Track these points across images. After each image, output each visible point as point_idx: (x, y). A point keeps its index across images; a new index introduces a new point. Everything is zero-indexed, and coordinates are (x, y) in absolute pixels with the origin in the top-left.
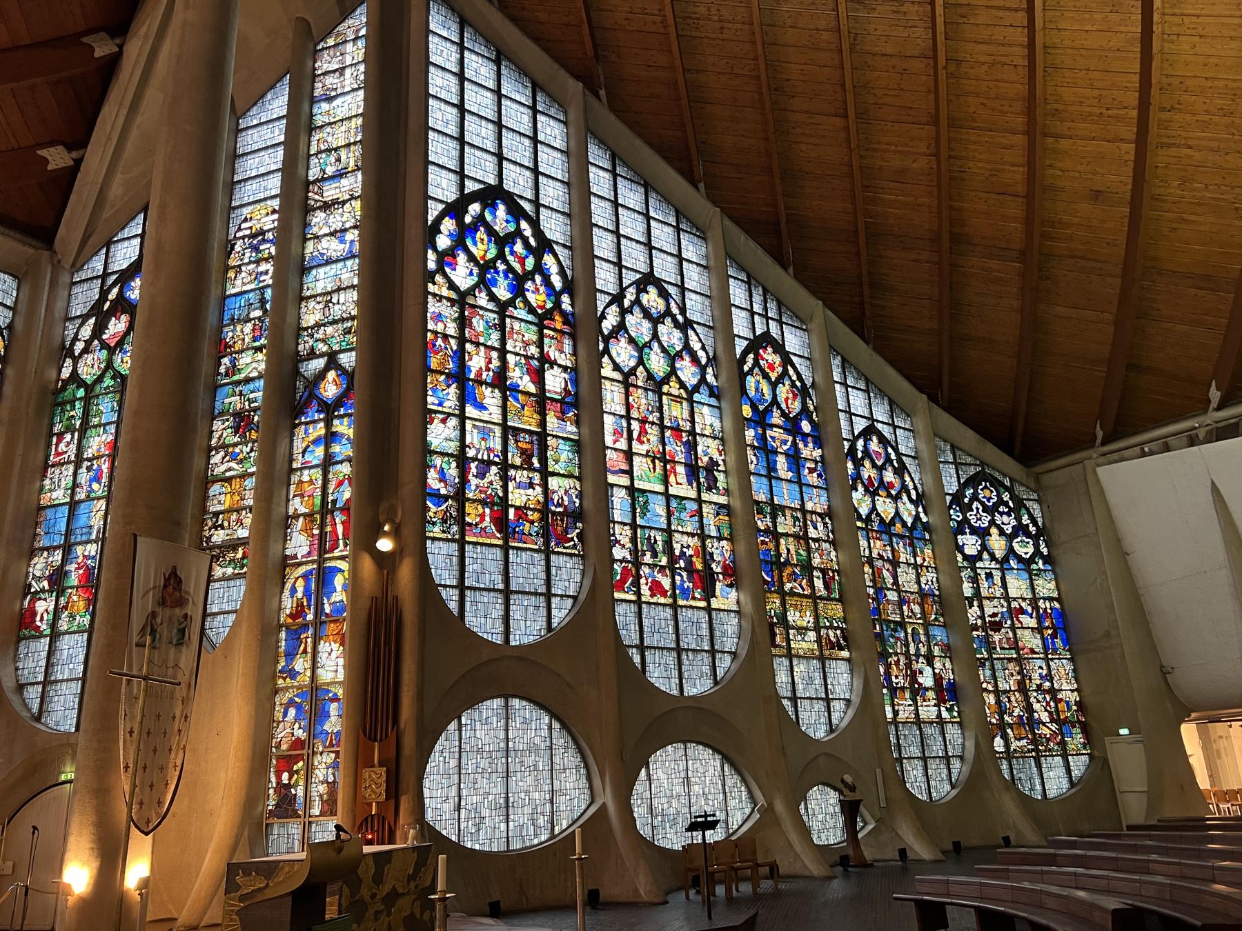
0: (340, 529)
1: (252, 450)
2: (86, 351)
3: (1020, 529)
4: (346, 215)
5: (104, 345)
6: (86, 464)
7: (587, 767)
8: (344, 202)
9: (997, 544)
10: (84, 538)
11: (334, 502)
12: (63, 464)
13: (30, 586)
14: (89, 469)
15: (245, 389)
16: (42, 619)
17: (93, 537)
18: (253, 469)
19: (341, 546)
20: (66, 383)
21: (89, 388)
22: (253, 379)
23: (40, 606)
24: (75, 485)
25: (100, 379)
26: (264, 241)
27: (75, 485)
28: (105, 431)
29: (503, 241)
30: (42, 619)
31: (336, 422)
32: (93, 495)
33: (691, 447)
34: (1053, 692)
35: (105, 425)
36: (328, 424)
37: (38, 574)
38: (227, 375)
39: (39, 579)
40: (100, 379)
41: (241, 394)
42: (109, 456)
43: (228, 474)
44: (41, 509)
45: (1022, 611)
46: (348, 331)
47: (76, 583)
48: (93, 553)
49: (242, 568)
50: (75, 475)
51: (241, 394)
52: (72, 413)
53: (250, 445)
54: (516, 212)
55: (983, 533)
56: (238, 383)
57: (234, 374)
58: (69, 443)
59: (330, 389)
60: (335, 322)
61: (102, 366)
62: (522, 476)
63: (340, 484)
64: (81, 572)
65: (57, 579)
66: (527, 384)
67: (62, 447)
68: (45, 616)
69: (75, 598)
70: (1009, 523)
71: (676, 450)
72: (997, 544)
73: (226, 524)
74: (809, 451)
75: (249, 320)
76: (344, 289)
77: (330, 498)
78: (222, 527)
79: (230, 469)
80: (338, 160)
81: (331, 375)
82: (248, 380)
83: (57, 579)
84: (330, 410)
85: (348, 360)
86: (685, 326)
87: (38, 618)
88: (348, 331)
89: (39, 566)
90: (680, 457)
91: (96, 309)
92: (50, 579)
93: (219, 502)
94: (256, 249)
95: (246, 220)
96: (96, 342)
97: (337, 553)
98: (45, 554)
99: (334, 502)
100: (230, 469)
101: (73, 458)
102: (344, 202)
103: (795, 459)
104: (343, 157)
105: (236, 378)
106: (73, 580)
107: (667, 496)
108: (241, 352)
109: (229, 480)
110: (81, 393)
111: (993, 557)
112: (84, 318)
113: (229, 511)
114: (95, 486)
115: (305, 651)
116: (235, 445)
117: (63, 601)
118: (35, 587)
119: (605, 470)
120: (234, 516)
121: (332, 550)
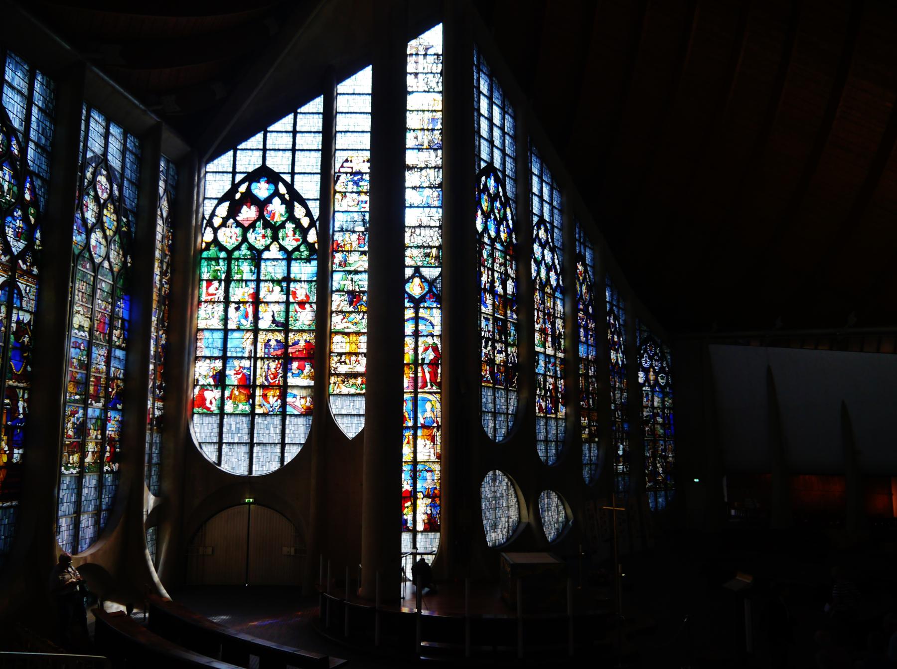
0: (428, 376)
1: (363, 318)
2: (224, 224)
3: (662, 370)
4: (423, 178)
5: (239, 224)
6: (233, 306)
7: (519, 504)
8: (422, 169)
9: (652, 377)
10: (240, 355)
11: (423, 359)
12: (214, 302)
13: (198, 380)
14: (237, 309)
15: (356, 277)
16: (211, 403)
18: (365, 330)
19: (429, 386)
21: (230, 253)
22: (361, 272)
24: (226, 319)
25: (238, 248)
26: (362, 179)
27: (226, 319)
28: (247, 286)
29: (493, 199)
30: (211, 403)
31: (421, 310)
32: (242, 327)
33: (553, 324)
34: (666, 457)
35: (246, 281)
36: (417, 312)
38: (340, 265)
40: (238, 248)
41: (352, 280)
42: (252, 303)
43: (346, 330)
44: (198, 330)
45: (658, 414)
46: (427, 255)
47: (236, 383)
49: (362, 389)
50: (226, 311)
51: (352, 280)
52: (217, 268)
53: (361, 314)
54: (497, 180)
55: (646, 371)
56: (350, 272)
57: (345, 266)
59: (415, 288)
60: (418, 247)
61: (240, 239)
62: (498, 346)
63: (426, 349)
64: (239, 376)
65: (220, 379)
66: (499, 290)
67: (212, 290)
68: (213, 401)
70: (657, 365)
71: (549, 326)
72: (652, 377)
73: (347, 361)
74: (592, 325)
75: (354, 232)
76: (425, 227)
77: (420, 357)
78: (346, 363)
79: (348, 328)
80: (416, 138)
81: (417, 280)
82: (356, 272)
83: (220, 379)
84: (417, 303)
85: (432, 273)
86: (552, 250)
88: (427, 255)
90: (549, 332)
91: (229, 196)
92: (214, 377)
93: (342, 347)
94: (356, 183)
95: (347, 161)
96: (231, 221)
97: (426, 389)
99: (423, 359)
100: (348, 328)
101: (222, 299)
102: (422, 169)
103: (586, 327)
104: (420, 138)
105: (347, 269)
107: (544, 353)
108: (350, 252)
109: (348, 334)
110: (223, 255)
111: (649, 386)
112: (221, 201)
113: (350, 354)
114: (243, 321)
115: (408, 443)
116: (350, 312)
117: (227, 393)
118: (202, 382)
119: (534, 345)
120: (353, 358)
121: (423, 387)
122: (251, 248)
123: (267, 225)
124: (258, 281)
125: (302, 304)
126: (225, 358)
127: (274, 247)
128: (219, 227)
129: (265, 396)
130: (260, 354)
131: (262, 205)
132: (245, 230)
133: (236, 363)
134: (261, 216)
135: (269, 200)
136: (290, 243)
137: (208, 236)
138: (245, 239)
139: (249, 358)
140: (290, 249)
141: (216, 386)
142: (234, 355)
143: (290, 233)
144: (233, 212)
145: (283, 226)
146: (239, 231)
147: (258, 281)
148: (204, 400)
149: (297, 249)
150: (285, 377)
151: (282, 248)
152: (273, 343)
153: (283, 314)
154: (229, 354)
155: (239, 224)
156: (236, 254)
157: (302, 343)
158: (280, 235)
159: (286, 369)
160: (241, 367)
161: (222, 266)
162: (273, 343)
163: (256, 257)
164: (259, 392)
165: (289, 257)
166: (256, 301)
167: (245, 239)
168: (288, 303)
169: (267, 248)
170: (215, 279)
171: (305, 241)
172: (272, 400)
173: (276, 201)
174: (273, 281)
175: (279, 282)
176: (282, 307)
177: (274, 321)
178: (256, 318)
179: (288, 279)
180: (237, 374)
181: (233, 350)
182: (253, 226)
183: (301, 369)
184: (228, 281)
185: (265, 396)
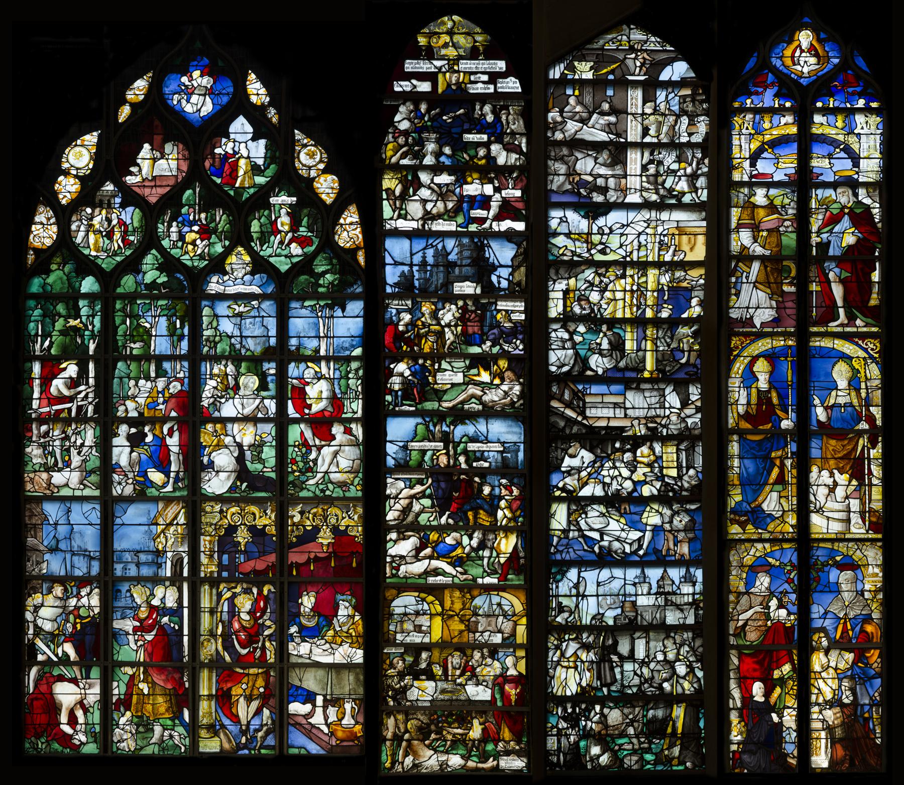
5: (130, 198)
10: (146, 571)
12: (68, 422)
14: (135, 441)
17: (167, 571)
20: (45, 256)
21: (109, 280)
23: (66, 694)
24: (107, 468)
37: (48, 626)
39: (53, 638)
48: (171, 603)
50: (104, 446)
58: (73, 383)
65: (95, 644)
67: (58, 385)
69: (144, 687)
83: (95, 644)
87: (64, 718)
89: (45, 612)
92: (76, 639)
98: (58, 590)
106: (131, 650)
110: (89, 285)
114: (156, 477)
118: (44, 652)
122: (169, 264)
123: (213, 199)
124: (195, 358)
125: (322, 426)
126: (108, 585)
127: (239, 261)
128: (77, 204)
129: (224, 700)
130: (208, 567)
131: (199, 138)
132: (152, 214)
133: (139, 595)
134: (194, 174)
135: (218, 126)
136: (284, 253)
137: (43, 232)
138: (150, 240)
139: (176, 580)
140: (283, 265)
141: (85, 664)
142: (133, 571)
143: (284, 222)
144: (114, 161)
145: (261, 199)
146: (132, 216)
147: (195, 358)
148: (54, 708)
149: (305, 266)
150: (282, 640)
151: (260, 265)
152: (242, 537)
153: (269, 453)
154: (118, 569)
155: (130, 198)
156: (128, 283)
157: (325, 538)
158: (255, 226)
159: (287, 613)
160: (152, 609)
161: (89, 318)
162: (242, 537)
163: (187, 291)
164: (206, 685)
165: (285, 289)
166: (192, 414)
167: (150, 240)
168: (282, 422)
169: (217, 265)
170: (67, 354)
171: (328, 243)
172: (244, 710)
173: (241, 126)
174: (236, 357)
175: (255, 363)
176: (268, 430)
177: (242, 472)
178: (195, 464)
179: (282, 352)
180: (143, 628)
181: (128, 557)
182: (171, 202)
183: (326, 612)
184: (109, 354)
185: (224, 700)
